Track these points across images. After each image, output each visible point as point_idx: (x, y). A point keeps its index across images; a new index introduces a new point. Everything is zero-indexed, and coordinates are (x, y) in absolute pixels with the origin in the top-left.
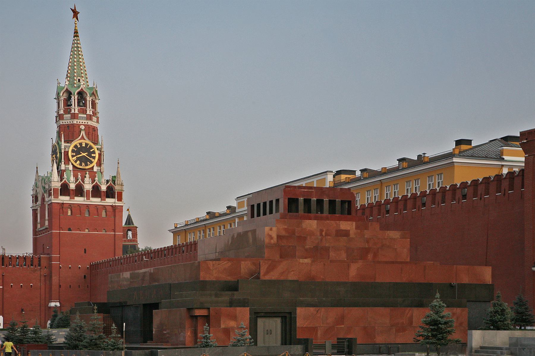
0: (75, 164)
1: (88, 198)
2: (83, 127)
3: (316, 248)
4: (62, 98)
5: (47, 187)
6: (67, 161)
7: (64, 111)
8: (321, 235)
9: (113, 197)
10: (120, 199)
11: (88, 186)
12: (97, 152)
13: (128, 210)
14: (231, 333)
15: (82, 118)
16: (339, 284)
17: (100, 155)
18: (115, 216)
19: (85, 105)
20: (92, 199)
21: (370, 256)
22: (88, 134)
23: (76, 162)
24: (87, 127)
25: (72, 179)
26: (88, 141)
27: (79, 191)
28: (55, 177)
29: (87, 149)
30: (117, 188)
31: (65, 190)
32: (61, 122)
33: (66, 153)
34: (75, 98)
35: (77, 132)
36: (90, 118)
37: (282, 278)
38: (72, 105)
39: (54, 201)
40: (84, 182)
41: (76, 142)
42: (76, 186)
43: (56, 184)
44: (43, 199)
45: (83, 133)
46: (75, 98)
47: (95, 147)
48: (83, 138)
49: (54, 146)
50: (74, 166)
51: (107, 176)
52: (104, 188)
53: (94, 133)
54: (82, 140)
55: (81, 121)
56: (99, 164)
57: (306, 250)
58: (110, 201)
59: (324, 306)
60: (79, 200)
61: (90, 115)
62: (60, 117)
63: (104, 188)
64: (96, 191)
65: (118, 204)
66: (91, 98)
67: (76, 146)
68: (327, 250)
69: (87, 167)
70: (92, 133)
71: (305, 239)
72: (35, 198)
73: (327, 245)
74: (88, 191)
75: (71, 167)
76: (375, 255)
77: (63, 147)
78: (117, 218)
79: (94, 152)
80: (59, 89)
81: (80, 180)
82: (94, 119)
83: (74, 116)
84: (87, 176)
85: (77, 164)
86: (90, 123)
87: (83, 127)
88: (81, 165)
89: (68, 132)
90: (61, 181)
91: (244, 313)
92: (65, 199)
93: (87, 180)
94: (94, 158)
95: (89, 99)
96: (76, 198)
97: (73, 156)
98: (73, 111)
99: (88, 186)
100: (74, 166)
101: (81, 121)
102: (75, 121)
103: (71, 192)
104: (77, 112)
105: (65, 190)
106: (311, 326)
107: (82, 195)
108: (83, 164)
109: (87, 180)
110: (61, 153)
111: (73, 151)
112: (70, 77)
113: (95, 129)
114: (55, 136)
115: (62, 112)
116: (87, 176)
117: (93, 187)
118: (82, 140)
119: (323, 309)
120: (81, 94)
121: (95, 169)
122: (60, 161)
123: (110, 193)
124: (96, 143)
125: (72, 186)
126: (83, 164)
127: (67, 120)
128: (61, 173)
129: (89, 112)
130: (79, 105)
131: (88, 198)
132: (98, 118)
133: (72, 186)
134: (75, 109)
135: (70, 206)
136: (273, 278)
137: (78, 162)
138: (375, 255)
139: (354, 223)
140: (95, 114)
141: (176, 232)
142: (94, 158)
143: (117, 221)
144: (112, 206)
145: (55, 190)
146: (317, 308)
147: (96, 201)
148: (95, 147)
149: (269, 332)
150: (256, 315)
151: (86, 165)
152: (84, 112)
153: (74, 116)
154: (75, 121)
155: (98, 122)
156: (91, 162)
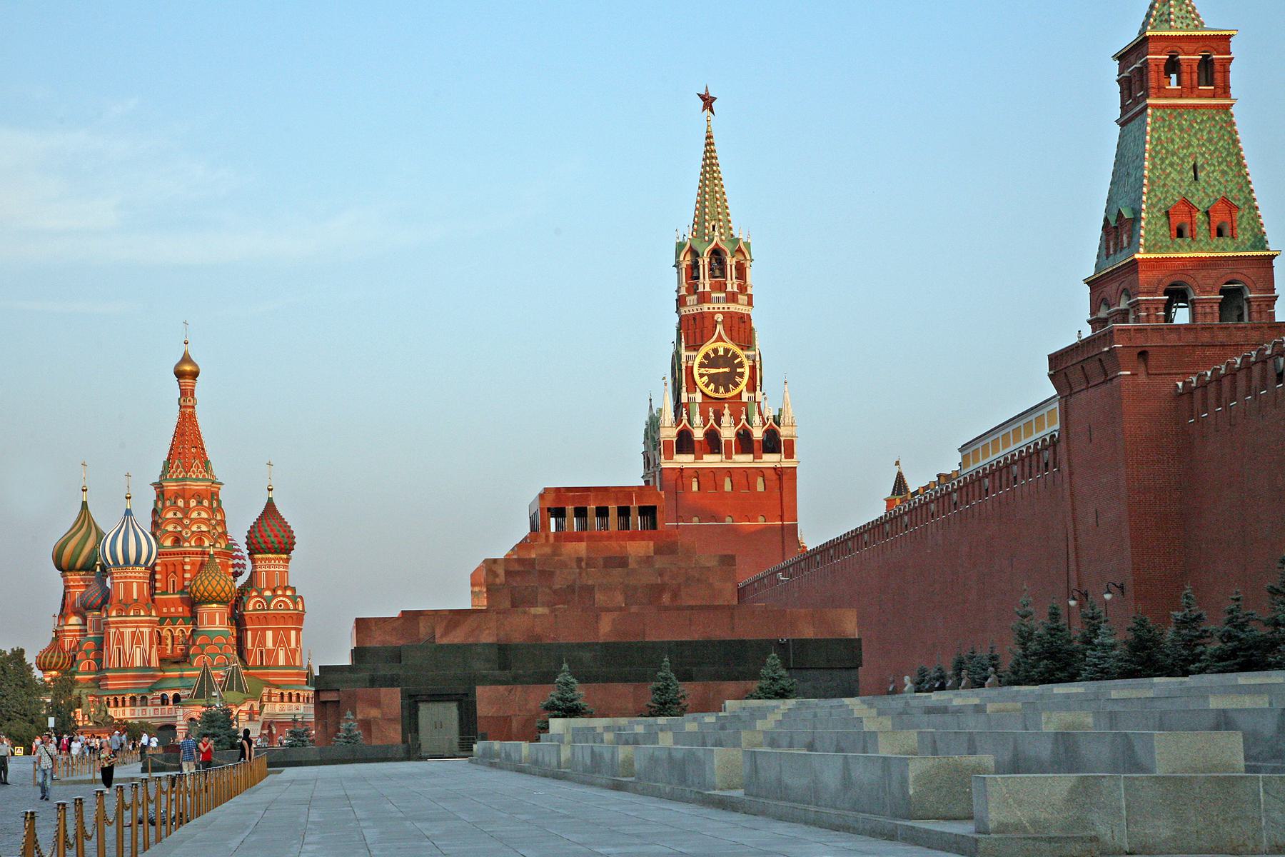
0: (707, 391)
1: (729, 457)
2: (719, 318)
3: (571, 588)
4: (684, 266)
6: (692, 386)
7: (687, 290)
8: (579, 567)
9: (775, 450)
10: (790, 454)
11: (728, 433)
12: (747, 364)
13: (897, 463)
14: (373, 728)
15: (718, 300)
16: (581, 646)
17: (753, 368)
18: (781, 488)
19: (724, 275)
20: (736, 457)
21: (666, 598)
22: (729, 330)
23: (707, 386)
24: (729, 316)
25: (697, 419)
26: (730, 345)
27: (713, 442)
29: (728, 359)
30: (784, 432)
31: (684, 443)
32: (684, 311)
33: (690, 370)
34: (704, 261)
35: (710, 327)
36: (732, 298)
37: (471, 640)
38: (698, 278)
39: (666, 464)
40: (719, 425)
41: (707, 348)
42: (706, 434)
43: (669, 432)
45: (719, 328)
46: (704, 261)
47: (743, 355)
48: (720, 339)
51: (770, 412)
52: (758, 434)
53: (742, 325)
54: (719, 344)
55: (717, 307)
56: (752, 387)
57: (555, 592)
58: (770, 460)
59: (521, 683)
60: (712, 461)
61: (734, 293)
62: (681, 302)
63: (758, 434)
64: (744, 442)
65: (786, 463)
66: (734, 260)
67: (706, 356)
68: (590, 590)
69: (728, 395)
70: (741, 329)
71: (551, 574)
73: (590, 582)
74: (728, 442)
75: (698, 397)
76: (675, 595)
77: (684, 360)
78: (785, 491)
79: (741, 365)
80: (680, 246)
81: (712, 421)
82: (743, 299)
84: (727, 412)
85: (709, 391)
86: (733, 307)
87: (719, 318)
88: (716, 391)
89: (693, 330)
90: (678, 426)
91: (393, 698)
92: (685, 460)
94: (741, 375)
95: (730, 261)
96: (707, 458)
97: (701, 376)
98: (701, 289)
99: (728, 433)
101: (716, 306)
102: (705, 308)
103: (697, 446)
104: (707, 289)
105: (684, 443)
106: (501, 714)
108: (721, 389)
109: (726, 419)
110: (680, 370)
112: (699, 222)
113: (744, 320)
115: (683, 292)
116: (727, 412)
117: (738, 434)
118: (719, 344)
119: (519, 688)
120: (717, 253)
121: (745, 397)
123: (772, 443)
125: (699, 434)
126: (721, 389)
127: (692, 307)
129: (732, 285)
130: (712, 276)
131: (729, 457)
132: (750, 297)
133: (699, 434)
134: (705, 284)
135: (697, 473)
136: (456, 641)
137: (712, 386)
138: (675, 595)
139: (651, 544)
140: (743, 289)
142: (741, 375)
143: (785, 500)
144: (775, 469)
145: (668, 444)
146: (510, 687)
147: (743, 461)
148: (743, 355)
149: (438, 726)
150: (412, 703)
151: (727, 390)
152: (722, 287)
153: (704, 298)
154: (705, 308)
155: (750, 303)
156: (736, 385)
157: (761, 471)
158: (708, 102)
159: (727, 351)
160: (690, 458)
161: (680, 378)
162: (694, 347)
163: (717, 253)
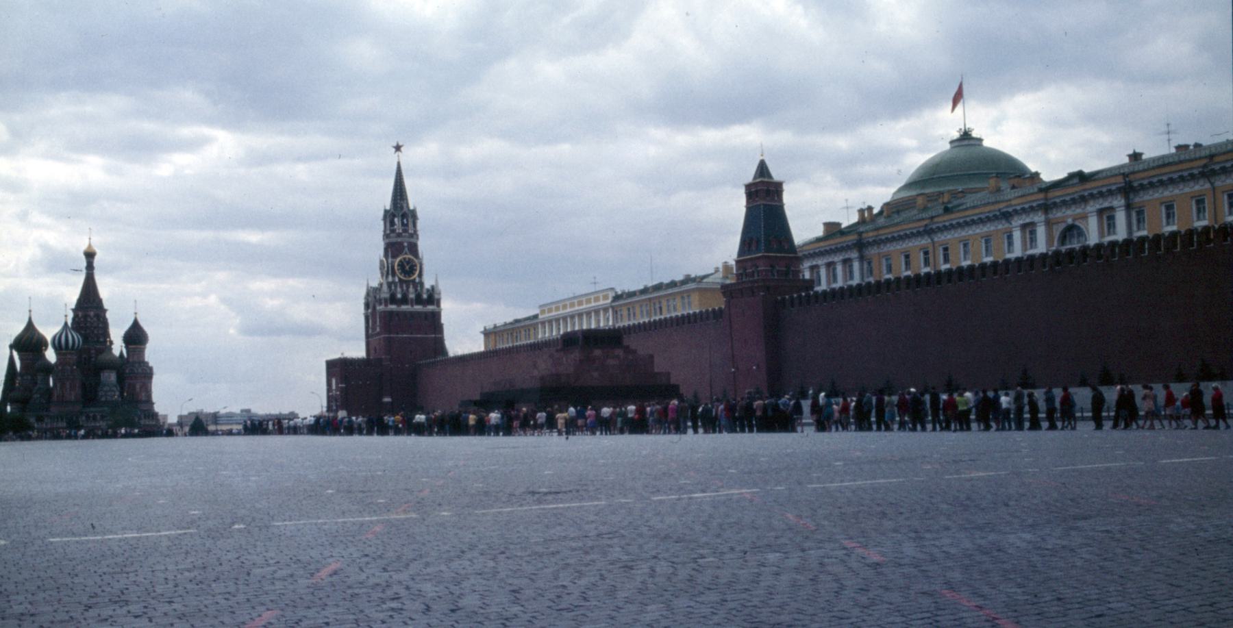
10: (438, 305)
11: (412, 296)
25: (399, 290)
27: (405, 300)
28: (385, 288)
30: (436, 296)
31: (393, 299)
36: (412, 236)
43: (385, 294)
44: (374, 308)
49: (381, 261)
51: (427, 285)
52: (425, 296)
56: (420, 275)
58: (430, 308)
60: (404, 308)
62: (386, 236)
63: (425, 296)
64: (419, 300)
70: (413, 249)
72: (367, 305)
83: (399, 235)
89: (392, 249)
92: (393, 307)
93: (411, 289)
99: (412, 296)
105: (393, 299)
109: (411, 289)
114: (382, 252)
125: (399, 296)
127: (394, 240)
128: (389, 285)
129: (411, 231)
133: (399, 296)
135: (398, 314)
140: (415, 231)
141: (487, 333)
145: (386, 300)
147: (418, 308)
158: (398, 148)
161: (387, 271)
162: (394, 257)
163: (404, 216)
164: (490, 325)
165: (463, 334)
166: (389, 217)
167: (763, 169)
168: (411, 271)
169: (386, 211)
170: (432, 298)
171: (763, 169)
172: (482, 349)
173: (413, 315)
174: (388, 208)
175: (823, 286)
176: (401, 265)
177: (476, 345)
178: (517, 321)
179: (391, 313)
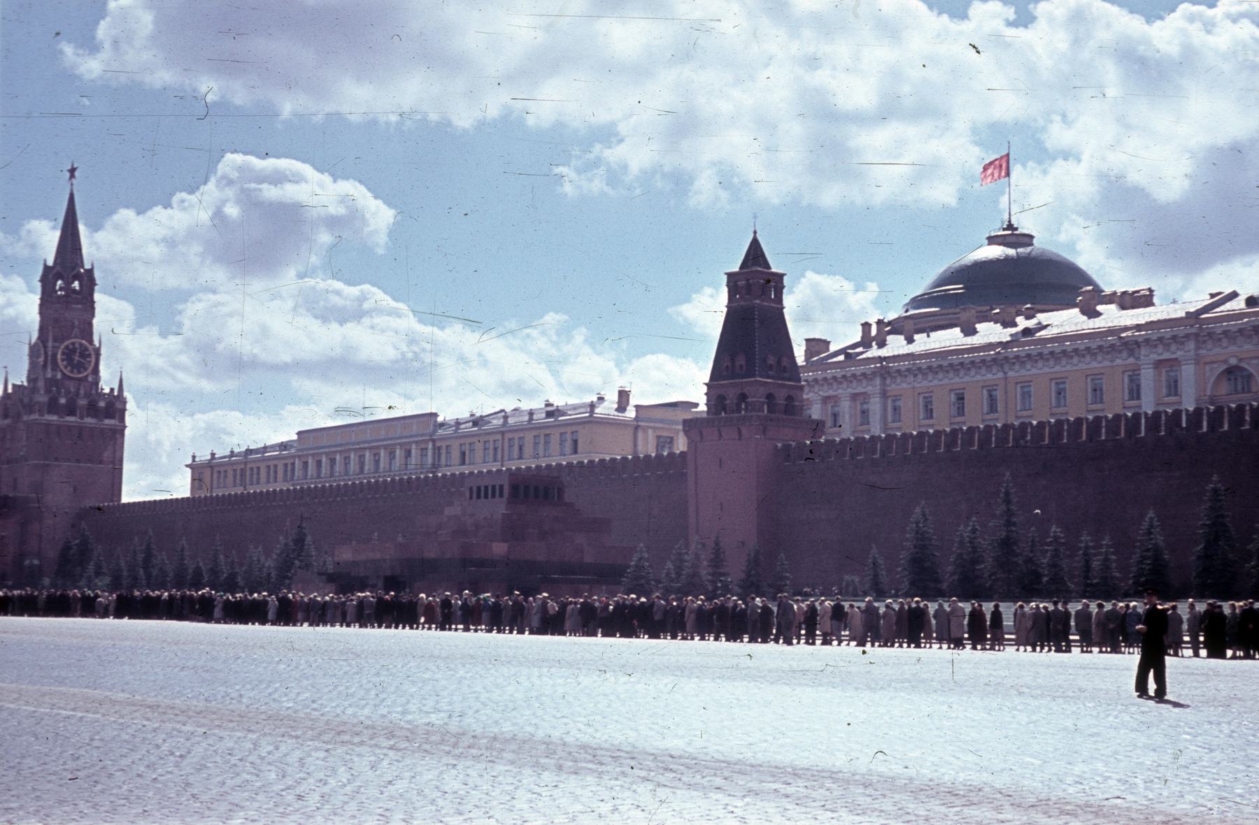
1: (82, 418)
5: (26, 400)
11: (82, 402)
30: (118, 405)
33: (54, 355)
43: (42, 398)
50: (64, 374)
52: (102, 404)
64: (92, 409)
67: (67, 347)
70: (87, 331)
75: (59, 376)
99: (82, 402)
100: (64, 374)
105: (53, 407)
107: (72, 413)
111: (63, 353)
121: (90, 379)
122: (45, 366)
124: (91, 341)
131: (82, 418)
147: (90, 421)
151: (79, 372)
156: (86, 369)
157: (102, 431)
159: (81, 345)
160: (54, 418)
164: (203, 456)
165: (155, 470)
166: (49, 276)
167: (755, 254)
168: (80, 367)
169: (46, 267)
170: (114, 407)
171: (755, 254)
172: (186, 493)
173: (81, 429)
174: (50, 263)
175: (847, 431)
176: (69, 353)
177: (180, 487)
178: (249, 452)
179: (48, 425)
